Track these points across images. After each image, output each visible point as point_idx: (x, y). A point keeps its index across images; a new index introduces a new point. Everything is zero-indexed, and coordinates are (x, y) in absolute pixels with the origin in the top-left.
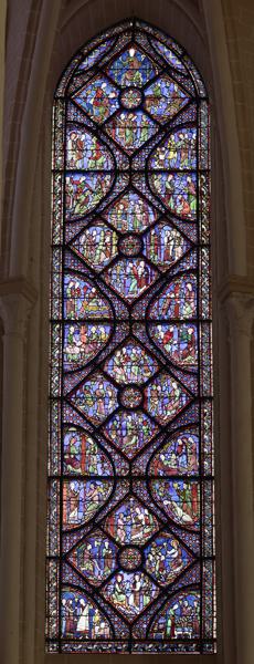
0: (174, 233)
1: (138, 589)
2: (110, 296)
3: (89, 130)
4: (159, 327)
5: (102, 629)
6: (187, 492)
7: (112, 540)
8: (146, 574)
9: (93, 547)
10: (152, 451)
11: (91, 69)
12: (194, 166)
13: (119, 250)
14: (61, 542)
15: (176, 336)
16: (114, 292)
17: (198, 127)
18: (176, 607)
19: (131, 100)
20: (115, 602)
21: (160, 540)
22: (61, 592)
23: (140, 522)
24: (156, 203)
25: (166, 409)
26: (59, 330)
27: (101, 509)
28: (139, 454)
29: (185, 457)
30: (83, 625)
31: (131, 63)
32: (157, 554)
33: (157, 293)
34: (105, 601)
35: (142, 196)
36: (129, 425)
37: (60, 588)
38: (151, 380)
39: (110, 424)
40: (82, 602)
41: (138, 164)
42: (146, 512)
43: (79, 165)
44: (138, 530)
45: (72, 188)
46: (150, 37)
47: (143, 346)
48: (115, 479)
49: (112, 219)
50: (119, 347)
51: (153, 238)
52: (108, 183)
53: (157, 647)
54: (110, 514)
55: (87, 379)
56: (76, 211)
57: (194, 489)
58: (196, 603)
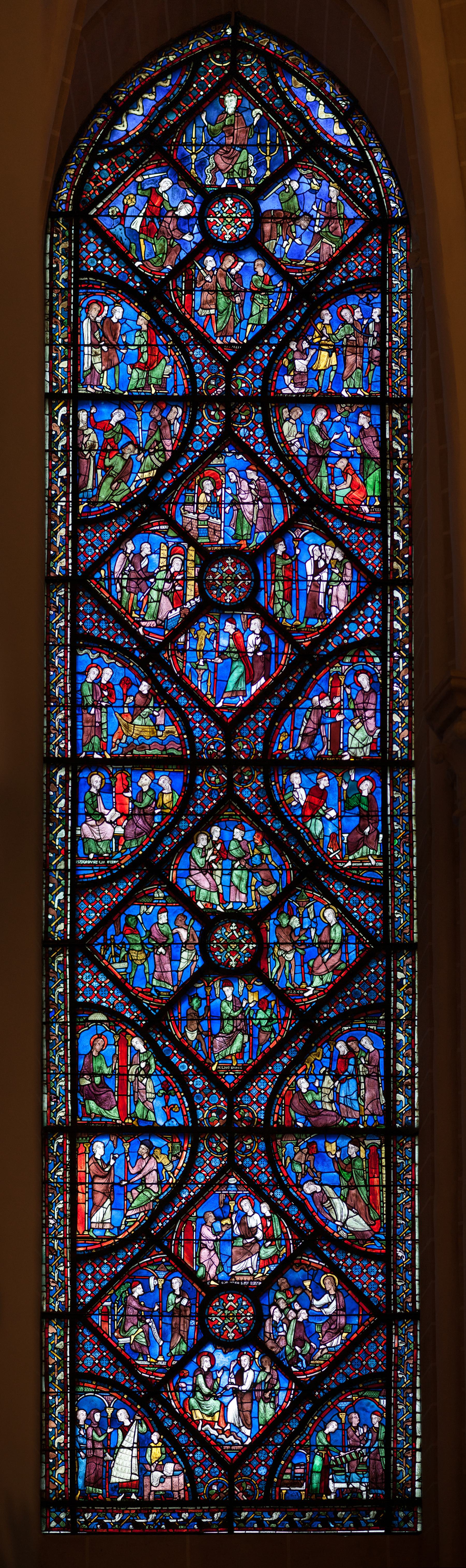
0: (329, 550)
1: (246, 1386)
2: (183, 701)
3: (132, 296)
4: (296, 778)
6: (358, 1164)
7: (188, 1274)
8: (266, 1352)
9: (146, 1289)
10: (279, 1069)
11: (135, 142)
12: (376, 390)
13: (201, 592)
14: (74, 1279)
15: (332, 798)
16: (193, 694)
17: (386, 292)
18: (332, 1427)
19: (229, 221)
21: (296, 1275)
22: (74, 1394)
23: (252, 1232)
24: (288, 478)
25: (312, 973)
27: (163, 1204)
28: (250, 1075)
29: (353, 1083)
30: (124, 1468)
31: (228, 130)
32: (290, 1306)
33: (291, 697)
34: (173, 1415)
36: (228, 1009)
37: (74, 1386)
38: (277, 903)
39: (185, 1006)
40: (122, 1415)
41: (246, 380)
42: (265, 1209)
44: (247, 1251)
45: (92, 437)
47: (256, 821)
48: (193, 1133)
49: (188, 517)
50: (204, 825)
51: (280, 563)
53: (289, 1519)
54: (184, 1214)
55: (131, 899)
56: (103, 495)
57: (373, 1157)
58: (375, 1419)
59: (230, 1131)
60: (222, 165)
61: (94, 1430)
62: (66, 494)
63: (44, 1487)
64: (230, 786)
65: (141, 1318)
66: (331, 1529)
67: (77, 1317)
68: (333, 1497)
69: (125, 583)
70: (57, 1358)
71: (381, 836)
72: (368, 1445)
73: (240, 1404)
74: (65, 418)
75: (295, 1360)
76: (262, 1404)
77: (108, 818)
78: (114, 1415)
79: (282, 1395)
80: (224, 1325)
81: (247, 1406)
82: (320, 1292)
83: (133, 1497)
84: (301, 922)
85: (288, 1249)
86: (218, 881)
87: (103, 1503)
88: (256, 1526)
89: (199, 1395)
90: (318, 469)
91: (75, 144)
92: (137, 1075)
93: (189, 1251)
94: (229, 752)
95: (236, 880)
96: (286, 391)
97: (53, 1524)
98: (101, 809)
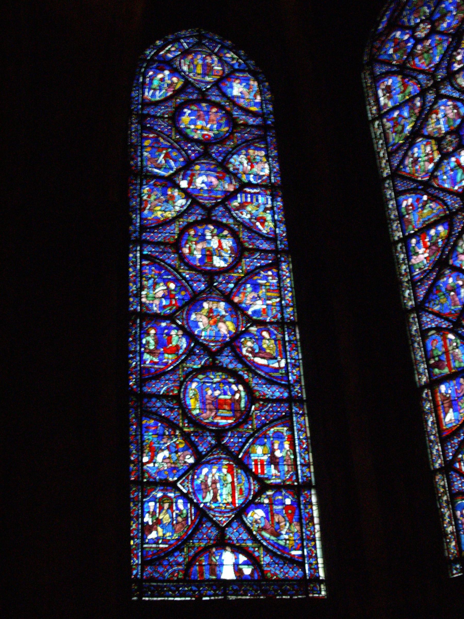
11: (385, 28)
14: (443, 450)
26: (401, 248)
35: (450, 98)
43: (390, 104)
45: (389, 125)
70: (442, 490)
74: (378, 125)
92: (453, 349)
96: (456, 69)
97: (455, 572)
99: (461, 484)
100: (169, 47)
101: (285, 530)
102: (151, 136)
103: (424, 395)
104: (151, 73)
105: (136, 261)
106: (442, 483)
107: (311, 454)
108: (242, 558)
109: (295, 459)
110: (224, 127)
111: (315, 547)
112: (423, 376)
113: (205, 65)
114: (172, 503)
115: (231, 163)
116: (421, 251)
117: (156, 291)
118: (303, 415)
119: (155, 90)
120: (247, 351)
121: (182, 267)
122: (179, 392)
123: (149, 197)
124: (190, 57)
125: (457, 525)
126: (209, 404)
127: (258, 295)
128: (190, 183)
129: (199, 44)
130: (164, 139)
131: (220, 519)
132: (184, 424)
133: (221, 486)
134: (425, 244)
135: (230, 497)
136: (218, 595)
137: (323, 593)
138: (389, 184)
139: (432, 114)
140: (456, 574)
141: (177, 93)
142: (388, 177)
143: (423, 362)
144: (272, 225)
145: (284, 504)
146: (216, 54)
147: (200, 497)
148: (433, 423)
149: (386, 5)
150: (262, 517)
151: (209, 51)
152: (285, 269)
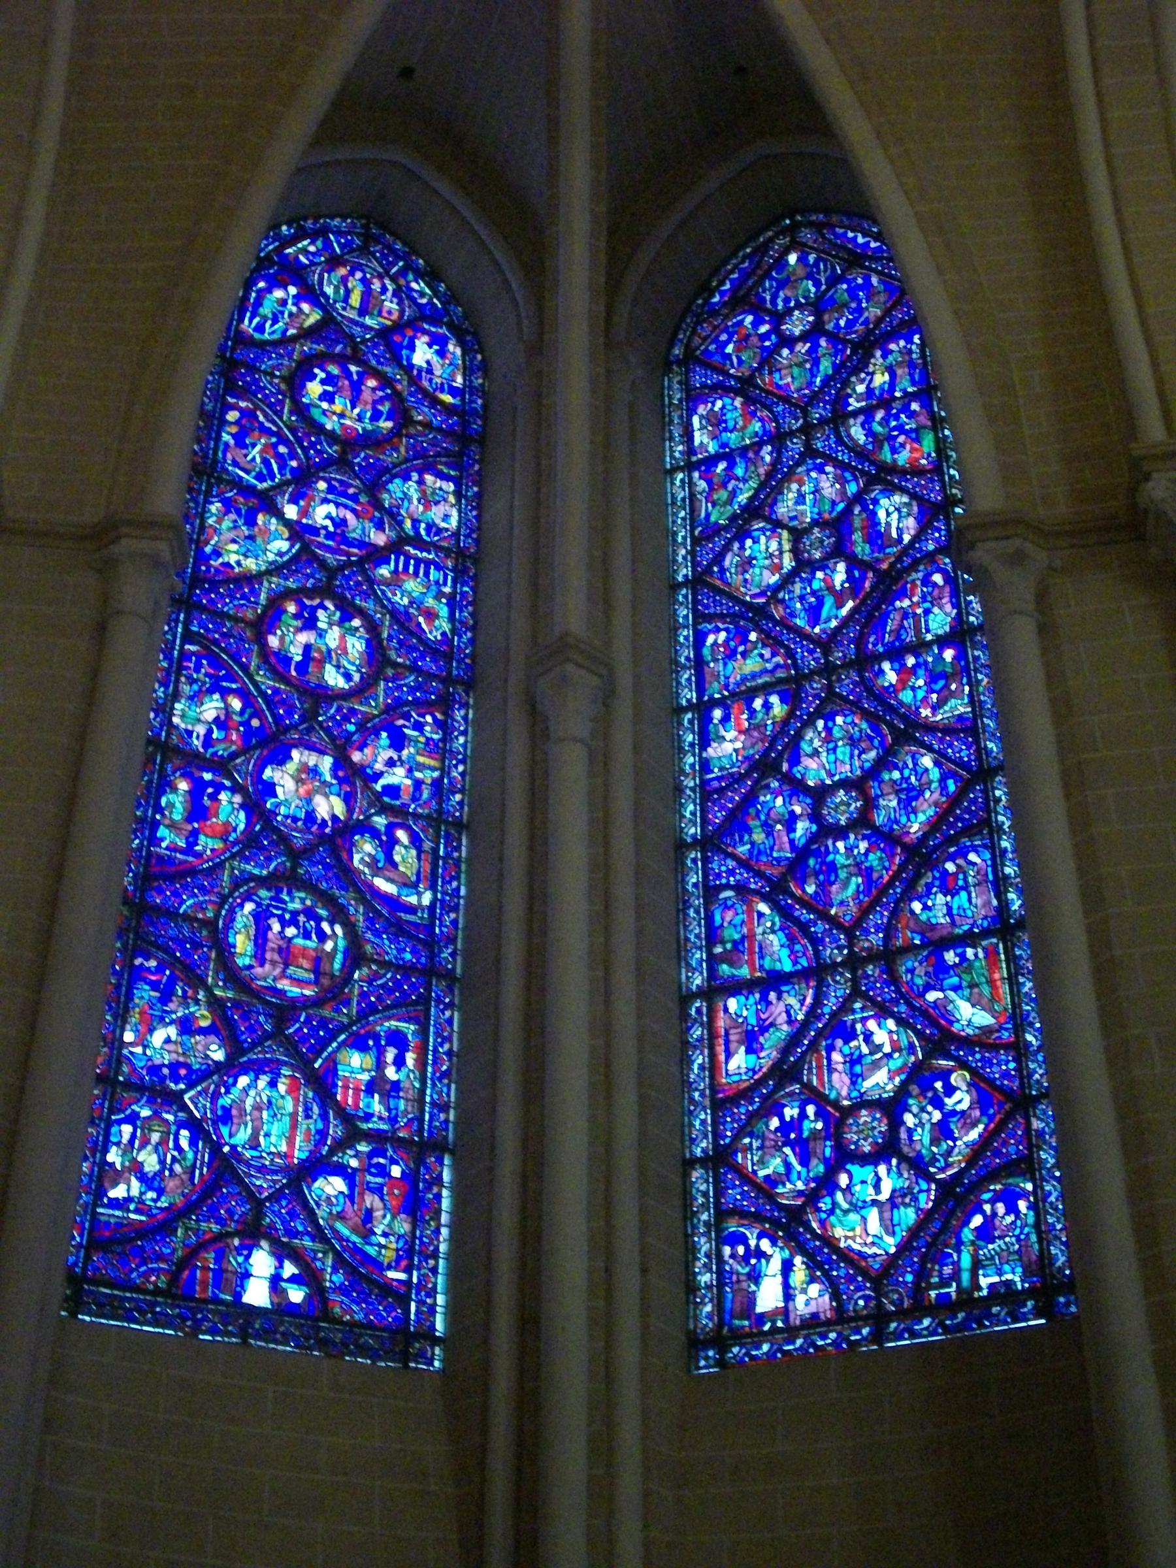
5: (812, 1298)
6: (977, 964)
8: (903, 1158)
20: (839, 1232)
23: (879, 1048)
26: (691, 722)
27: (793, 1040)
29: (963, 894)
30: (768, 1297)
34: (816, 1236)
42: (891, 1024)
43: (712, 447)
44: (876, 1065)
46: (818, 227)
52: (768, 458)
53: (941, 1324)
57: (991, 953)
59: (854, 962)
60: (789, 293)
61: (739, 1263)
62: (685, 527)
63: (692, 1327)
64: (829, 688)
65: (779, 1149)
66: (987, 1327)
67: (721, 1159)
68: (985, 1292)
69: (733, 570)
70: (701, 1200)
71: (967, 688)
72: (1017, 1232)
73: (881, 1213)
74: (682, 481)
75: (934, 1159)
76: (902, 1208)
77: (728, 738)
78: (757, 1246)
79: (922, 1197)
80: (858, 1140)
81: (887, 1215)
82: (950, 1090)
83: (780, 1324)
84: (902, 774)
85: (917, 1056)
86: (824, 760)
87: (750, 1335)
88: (906, 1335)
89: (838, 1211)
90: (881, 448)
91: (682, 319)
92: (764, 933)
93: (820, 1079)
94: (827, 662)
95: (840, 757)
97: (702, 1363)
98: (722, 732)
99: (740, 1194)
100: (305, 243)
101: (382, 1227)
102: (243, 404)
103: (693, 1012)
104: (262, 284)
105: (174, 641)
106: (703, 1187)
107: (453, 1086)
108: (289, 1269)
109: (422, 1092)
110: (386, 420)
111: (434, 1271)
112: (697, 974)
113: (367, 294)
114: (168, 1134)
115: (389, 491)
116: (731, 734)
117: (204, 707)
118: (450, 1006)
119: (265, 319)
120: (362, 860)
121: (261, 673)
122: (217, 916)
123: (219, 521)
124: (343, 271)
125: (720, 1273)
126: (273, 949)
127: (400, 757)
128: (304, 513)
129: (364, 250)
130: (266, 416)
131: (258, 1183)
132: (215, 979)
133: (270, 1120)
134: (738, 724)
135: (284, 1143)
136: (230, 1334)
137: (437, 1364)
138: (685, 596)
139: (790, 481)
140: (705, 1367)
141: (308, 334)
142: (686, 582)
143: (700, 948)
144: (446, 627)
145: (389, 1175)
146: (393, 279)
147: (225, 1131)
148: (702, 1067)
149: (734, 261)
150: (342, 1193)
151: (381, 270)
152: (459, 718)
